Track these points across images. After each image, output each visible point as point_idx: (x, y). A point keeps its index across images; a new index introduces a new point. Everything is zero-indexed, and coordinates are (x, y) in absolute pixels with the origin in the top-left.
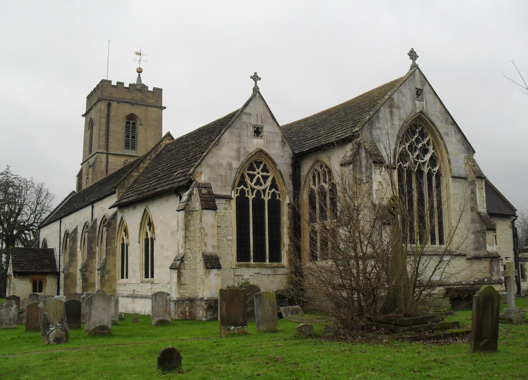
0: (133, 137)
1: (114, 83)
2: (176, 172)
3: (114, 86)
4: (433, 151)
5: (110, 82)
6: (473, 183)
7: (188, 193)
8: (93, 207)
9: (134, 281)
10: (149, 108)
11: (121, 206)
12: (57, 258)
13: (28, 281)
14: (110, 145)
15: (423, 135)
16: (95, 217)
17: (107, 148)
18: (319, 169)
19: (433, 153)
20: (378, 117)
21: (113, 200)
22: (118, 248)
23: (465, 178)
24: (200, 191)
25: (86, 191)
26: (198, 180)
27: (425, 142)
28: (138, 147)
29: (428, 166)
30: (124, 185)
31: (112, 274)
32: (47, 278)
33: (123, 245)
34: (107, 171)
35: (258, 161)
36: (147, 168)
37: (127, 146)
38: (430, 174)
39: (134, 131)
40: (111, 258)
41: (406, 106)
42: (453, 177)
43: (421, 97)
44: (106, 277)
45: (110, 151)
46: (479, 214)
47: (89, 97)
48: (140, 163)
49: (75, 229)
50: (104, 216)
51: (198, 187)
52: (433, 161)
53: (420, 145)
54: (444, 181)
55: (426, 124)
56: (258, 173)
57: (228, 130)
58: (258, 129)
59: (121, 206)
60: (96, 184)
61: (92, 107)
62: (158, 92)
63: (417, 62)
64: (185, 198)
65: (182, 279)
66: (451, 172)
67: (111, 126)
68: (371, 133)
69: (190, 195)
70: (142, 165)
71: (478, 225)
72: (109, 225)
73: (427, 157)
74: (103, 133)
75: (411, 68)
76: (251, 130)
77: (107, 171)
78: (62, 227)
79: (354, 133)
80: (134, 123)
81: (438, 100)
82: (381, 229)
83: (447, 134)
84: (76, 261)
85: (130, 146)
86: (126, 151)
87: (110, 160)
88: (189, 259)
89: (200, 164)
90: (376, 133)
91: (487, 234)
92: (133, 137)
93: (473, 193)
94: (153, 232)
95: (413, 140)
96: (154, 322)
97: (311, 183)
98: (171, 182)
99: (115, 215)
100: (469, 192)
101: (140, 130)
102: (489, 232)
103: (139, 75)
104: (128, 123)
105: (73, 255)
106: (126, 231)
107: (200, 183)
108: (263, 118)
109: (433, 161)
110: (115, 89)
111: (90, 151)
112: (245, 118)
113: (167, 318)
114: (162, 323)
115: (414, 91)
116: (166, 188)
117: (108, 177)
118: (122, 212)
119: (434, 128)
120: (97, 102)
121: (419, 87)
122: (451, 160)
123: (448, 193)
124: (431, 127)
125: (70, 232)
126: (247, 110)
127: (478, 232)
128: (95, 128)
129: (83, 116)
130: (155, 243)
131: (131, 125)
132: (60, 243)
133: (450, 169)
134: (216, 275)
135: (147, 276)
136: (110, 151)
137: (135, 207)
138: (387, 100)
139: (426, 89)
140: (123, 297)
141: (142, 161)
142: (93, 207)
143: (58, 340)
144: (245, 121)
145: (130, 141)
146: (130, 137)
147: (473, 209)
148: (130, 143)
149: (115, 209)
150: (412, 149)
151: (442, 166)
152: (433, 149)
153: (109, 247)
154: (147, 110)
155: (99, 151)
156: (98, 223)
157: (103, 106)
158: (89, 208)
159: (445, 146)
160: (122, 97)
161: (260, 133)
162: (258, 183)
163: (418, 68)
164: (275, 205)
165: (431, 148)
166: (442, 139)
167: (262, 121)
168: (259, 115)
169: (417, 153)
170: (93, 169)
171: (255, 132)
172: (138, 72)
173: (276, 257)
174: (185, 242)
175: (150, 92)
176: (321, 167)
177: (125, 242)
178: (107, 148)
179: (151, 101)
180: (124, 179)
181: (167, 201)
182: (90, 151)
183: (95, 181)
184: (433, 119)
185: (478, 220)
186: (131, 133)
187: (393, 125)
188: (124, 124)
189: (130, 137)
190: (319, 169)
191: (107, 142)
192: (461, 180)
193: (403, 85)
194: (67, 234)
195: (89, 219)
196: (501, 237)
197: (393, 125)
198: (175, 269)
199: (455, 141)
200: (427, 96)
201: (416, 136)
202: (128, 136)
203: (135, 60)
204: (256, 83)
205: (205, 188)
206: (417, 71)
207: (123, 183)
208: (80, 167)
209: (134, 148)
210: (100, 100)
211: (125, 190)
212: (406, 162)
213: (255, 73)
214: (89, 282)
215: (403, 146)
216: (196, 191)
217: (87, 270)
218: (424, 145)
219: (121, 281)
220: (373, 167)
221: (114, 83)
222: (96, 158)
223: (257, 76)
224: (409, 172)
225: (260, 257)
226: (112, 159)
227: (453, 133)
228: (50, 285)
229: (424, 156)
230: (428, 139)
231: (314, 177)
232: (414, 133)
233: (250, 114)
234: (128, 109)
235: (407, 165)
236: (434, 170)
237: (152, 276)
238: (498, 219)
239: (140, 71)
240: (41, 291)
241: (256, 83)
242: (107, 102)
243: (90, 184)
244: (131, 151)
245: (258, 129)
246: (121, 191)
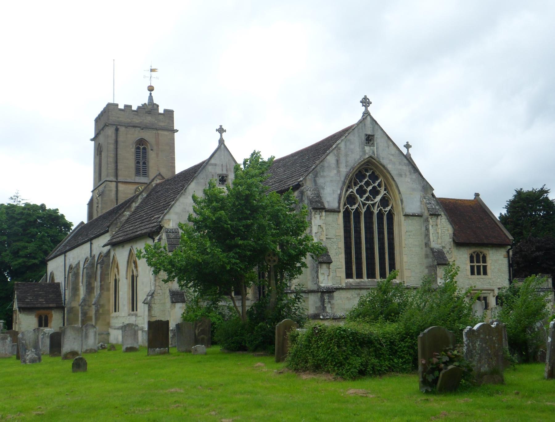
0: (144, 163)
1: (121, 107)
2: (153, 216)
3: (121, 110)
4: (385, 192)
5: (117, 105)
6: (427, 220)
7: (158, 238)
8: (91, 244)
9: (123, 314)
10: (160, 132)
11: (114, 244)
12: (63, 291)
13: (34, 317)
14: (120, 173)
15: (374, 177)
16: (93, 253)
17: (116, 176)
19: (385, 194)
20: (323, 166)
21: (106, 239)
22: (111, 283)
23: (420, 216)
24: (168, 237)
25: (96, 220)
26: (166, 226)
27: (376, 184)
28: (150, 174)
29: (378, 207)
30: (116, 224)
31: (106, 308)
32: (53, 312)
33: (116, 280)
34: (117, 200)
40: (105, 293)
41: (354, 154)
42: (406, 215)
43: (371, 143)
44: (101, 311)
45: (120, 179)
46: (432, 249)
47: (97, 120)
48: (132, 203)
49: (77, 264)
50: (100, 253)
51: (167, 232)
52: (385, 202)
53: (370, 188)
54: (396, 219)
55: (377, 167)
57: (195, 181)
58: (223, 177)
59: (114, 244)
60: (101, 216)
61: (100, 132)
62: (169, 114)
63: (369, 109)
64: (156, 241)
65: (153, 312)
66: (403, 211)
67: (119, 152)
68: (315, 181)
69: (160, 240)
70: (134, 204)
71: (430, 260)
72: (102, 263)
73: (378, 198)
74: (111, 160)
75: (363, 116)
77: (117, 200)
78: (67, 261)
79: (299, 182)
80: (144, 149)
81: (391, 143)
82: (318, 267)
83: (400, 175)
84: (78, 295)
85: (141, 173)
86: (137, 177)
88: (159, 295)
89: (168, 212)
90: (320, 181)
91: (438, 269)
92: (144, 163)
93: (427, 230)
94: (137, 270)
95: (363, 183)
96: (124, 348)
98: (147, 226)
99: (109, 252)
100: (424, 229)
101: (152, 156)
102: (440, 266)
103: (151, 94)
104: (138, 148)
105: (75, 289)
106: (117, 268)
107: (168, 229)
108: (228, 167)
109: (385, 202)
110: (123, 113)
111: (100, 179)
112: (210, 168)
113: (135, 345)
114: (130, 349)
115: (364, 138)
116: (144, 232)
117: (119, 206)
118: (114, 250)
119: (385, 171)
120: (104, 127)
121: (369, 133)
122: (404, 200)
123: (400, 231)
124: (381, 169)
125: (74, 266)
126: (212, 161)
127: (430, 266)
128: (103, 154)
129: (92, 140)
130: (138, 279)
131: (141, 151)
132: (65, 278)
133: (403, 208)
134: (180, 307)
135: (133, 310)
136: (120, 179)
137: (123, 246)
138: (333, 149)
139: (378, 135)
140: (115, 329)
141: (133, 202)
142: (91, 244)
143: (33, 361)
144: (210, 171)
145: (141, 167)
146: (141, 163)
147: (427, 245)
148: (141, 169)
149: (109, 247)
150: (361, 192)
151: (394, 206)
152: (385, 190)
153: (103, 283)
154: (158, 134)
155: (108, 179)
156: (96, 259)
157: (110, 131)
158: (88, 245)
159: (397, 187)
160: (130, 121)
161: (225, 181)
163: (369, 115)
165: (383, 188)
166: (394, 181)
167: (227, 170)
168: (224, 164)
169: (366, 195)
170: (102, 198)
171: (220, 180)
172: (149, 90)
174: (155, 280)
175: (161, 114)
177: (117, 278)
178: (116, 176)
179: (162, 124)
180: (116, 218)
182: (100, 179)
183: (105, 211)
184: (384, 162)
185: (431, 255)
186: (141, 159)
187: (339, 172)
188: (133, 150)
189: (141, 163)
191: (117, 169)
192: (415, 218)
193: (351, 133)
195: (88, 255)
196: (493, 267)
197: (339, 172)
198: (146, 303)
199: (409, 181)
200: (379, 140)
201: (366, 180)
203: (145, 77)
204: (221, 136)
205: (173, 232)
206: (369, 117)
207: (115, 222)
208: (91, 195)
209: (145, 174)
210: (106, 125)
211: (117, 229)
212: (355, 204)
213: (221, 126)
214: (88, 315)
215: (351, 190)
216: (164, 236)
217: (85, 305)
218: (374, 188)
219: (114, 314)
220: (313, 213)
221: (121, 107)
222: (105, 187)
223: (223, 129)
224: (357, 213)
226: (121, 187)
227: (408, 173)
229: (374, 198)
230: (379, 181)
232: (364, 176)
233: (216, 165)
234: (138, 134)
235: (355, 207)
236: (386, 210)
237: (137, 310)
238: (489, 249)
239: (151, 89)
240: (46, 325)
241: (221, 136)
242: (114, 127)
243: (100, 215)
244: (142, 178)
245: (223, 177)
246: (113, 230)
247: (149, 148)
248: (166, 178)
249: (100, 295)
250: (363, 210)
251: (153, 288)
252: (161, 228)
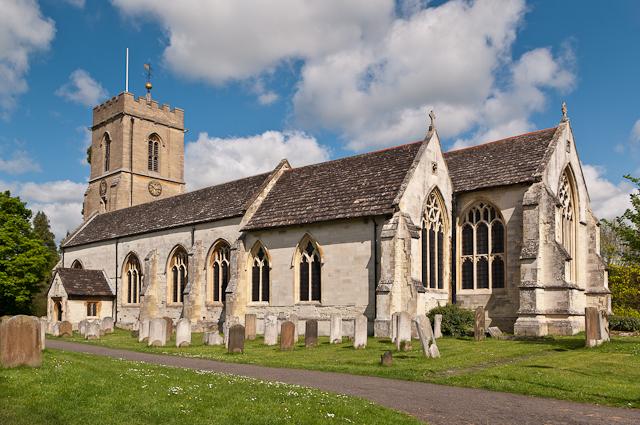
0: (156, 158)
18: (479, 208)
33: (256, 270)
36: (271, 193)
39: (156, 153)
76: (431, 166)
80: (156, 144)
87: (134, 181)
97: (467, 219)
101: (162, 151)
118: (256, 236)
162: (432, 216)
164: (441, 235)
173: (441, 286)
176: (482, 206)
181: (347, 227)
185: (597, 261)
188: (147, 143)
190: (479, 208)
202: (150, 157)
209: (156, 170)
216: (401, 220)
231: (471, 215)
234: (152, 128)
240: (95, 315)
247: (160, 146)
248: (293, 167)
252: (396, 207)
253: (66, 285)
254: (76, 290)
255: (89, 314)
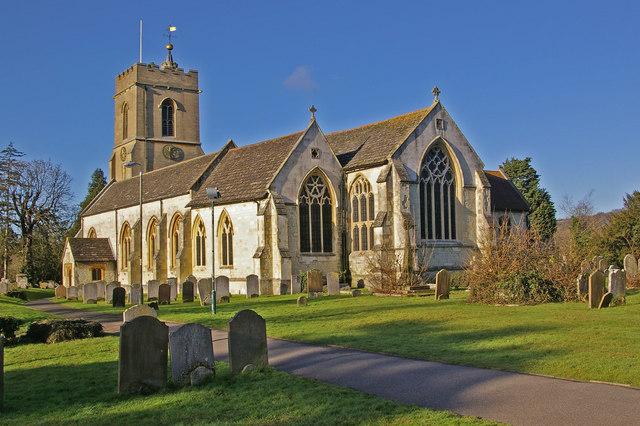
11: (193, 205)
21: (187, 199)
33: (198, 238)
35: (315, 177)
37: (164, 133)
38: (445, 186)
41: (429, 137)
56: (315, 185)
59: (193, 205)
69: (268, 203)
78: (119, 218)
94: (231, 229)
164: (328, 209)
173: (328, 248)
194: (126, 226)
195: (157, 212)
216: (272, 201)
225: (317, 248)
228: (107, 275)
232: (434, 154)
249: (184, 251)
250: (433, 183)
251: (262, 245)
253: (76, 254)
254: (82, 258)
255: (94, 278)
